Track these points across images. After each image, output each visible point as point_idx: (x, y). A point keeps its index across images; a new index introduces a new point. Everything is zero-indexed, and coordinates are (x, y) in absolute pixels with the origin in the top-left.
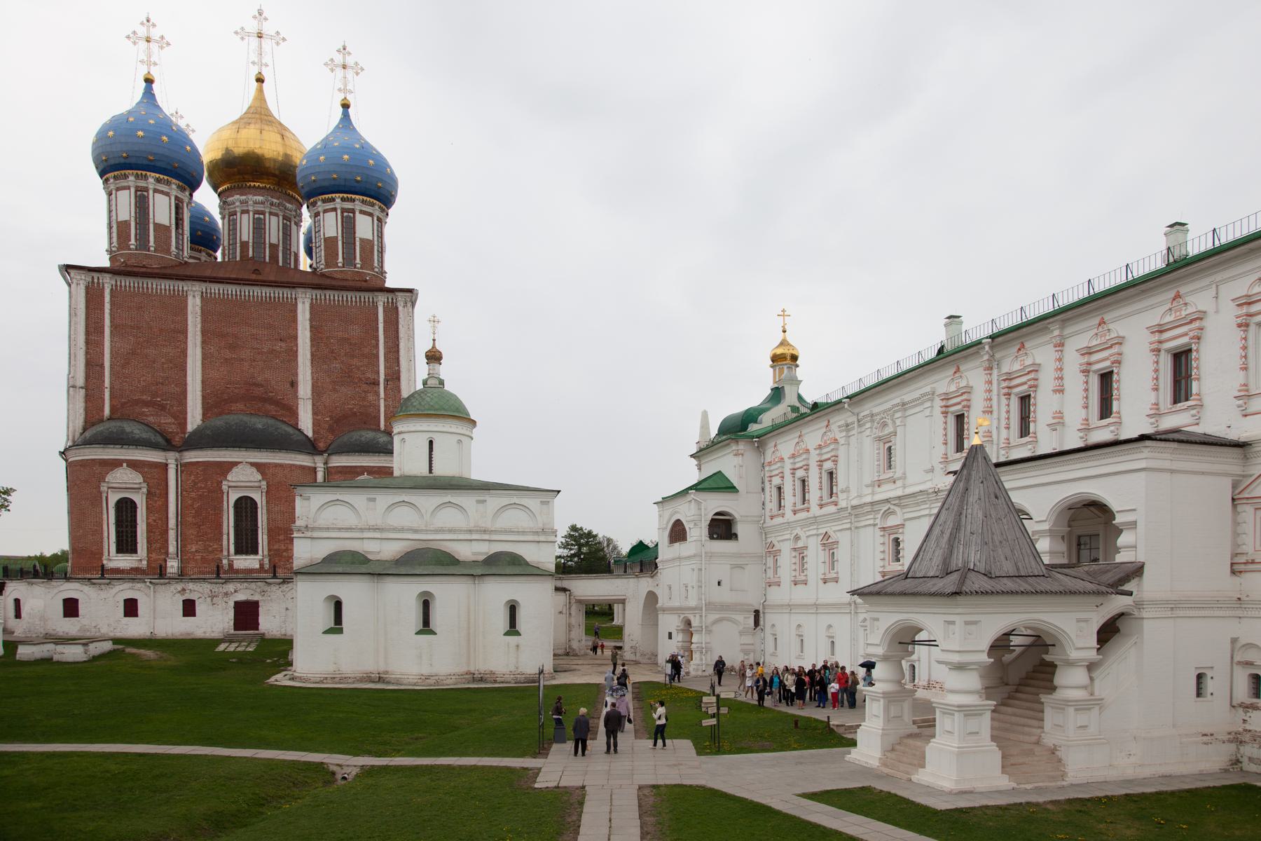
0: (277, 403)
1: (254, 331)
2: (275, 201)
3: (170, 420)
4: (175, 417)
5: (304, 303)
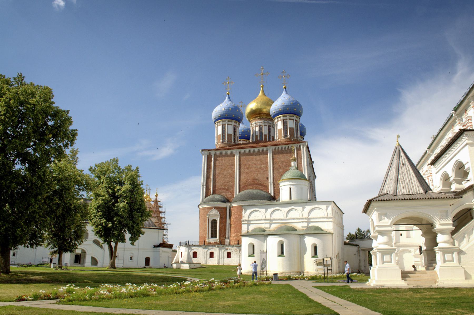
0: (262, 185)
1: (255, 162)
2: (266, 121)
3: (230, 194)
4: (231, 192)
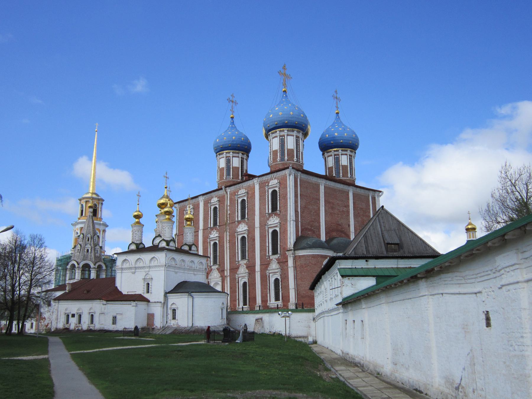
5: (351, 192)
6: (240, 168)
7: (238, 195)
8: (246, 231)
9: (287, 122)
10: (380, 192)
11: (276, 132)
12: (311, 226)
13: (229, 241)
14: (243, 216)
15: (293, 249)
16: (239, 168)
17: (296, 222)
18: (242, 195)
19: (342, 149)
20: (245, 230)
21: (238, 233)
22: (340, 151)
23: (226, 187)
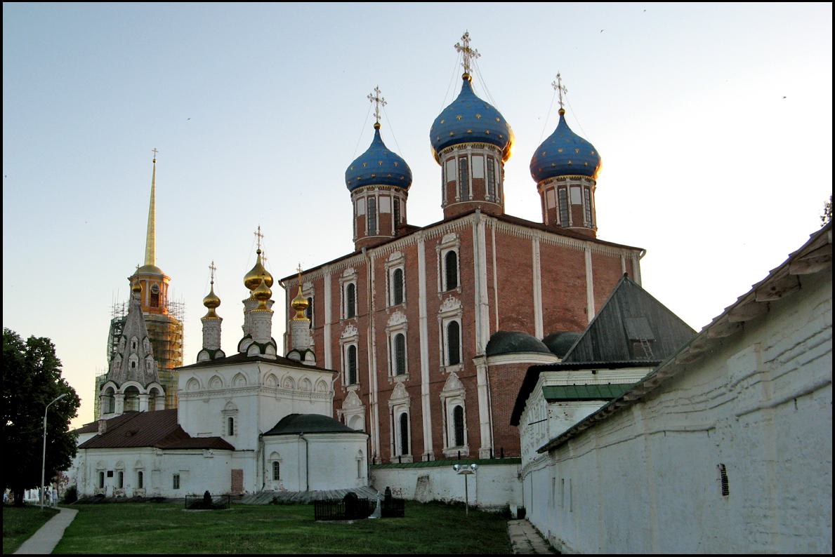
1: (565, 270)
6: (393, 215)
7: (389, 262)
8: (404, 324)
9: (469, 131)
10: (641, 250)
11: (453, 149)
12: (518, 314)
13: (376, 343)
14: (398, 299)
15: (485, 354)
16: (391, 214)
17: (490, 307)
18: (396, 262)
19: (571, 176)
20: (402, 323)
21: (391, 329)
22: (568, 180)
23: (367, 249)
